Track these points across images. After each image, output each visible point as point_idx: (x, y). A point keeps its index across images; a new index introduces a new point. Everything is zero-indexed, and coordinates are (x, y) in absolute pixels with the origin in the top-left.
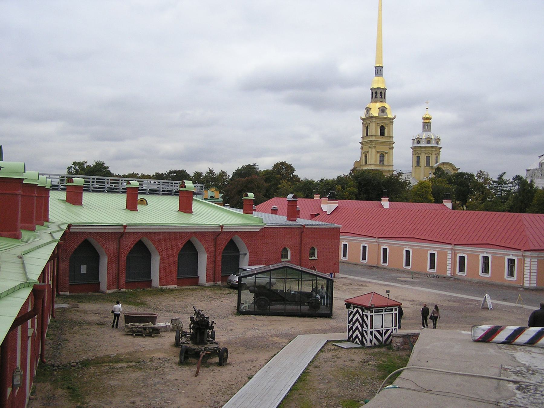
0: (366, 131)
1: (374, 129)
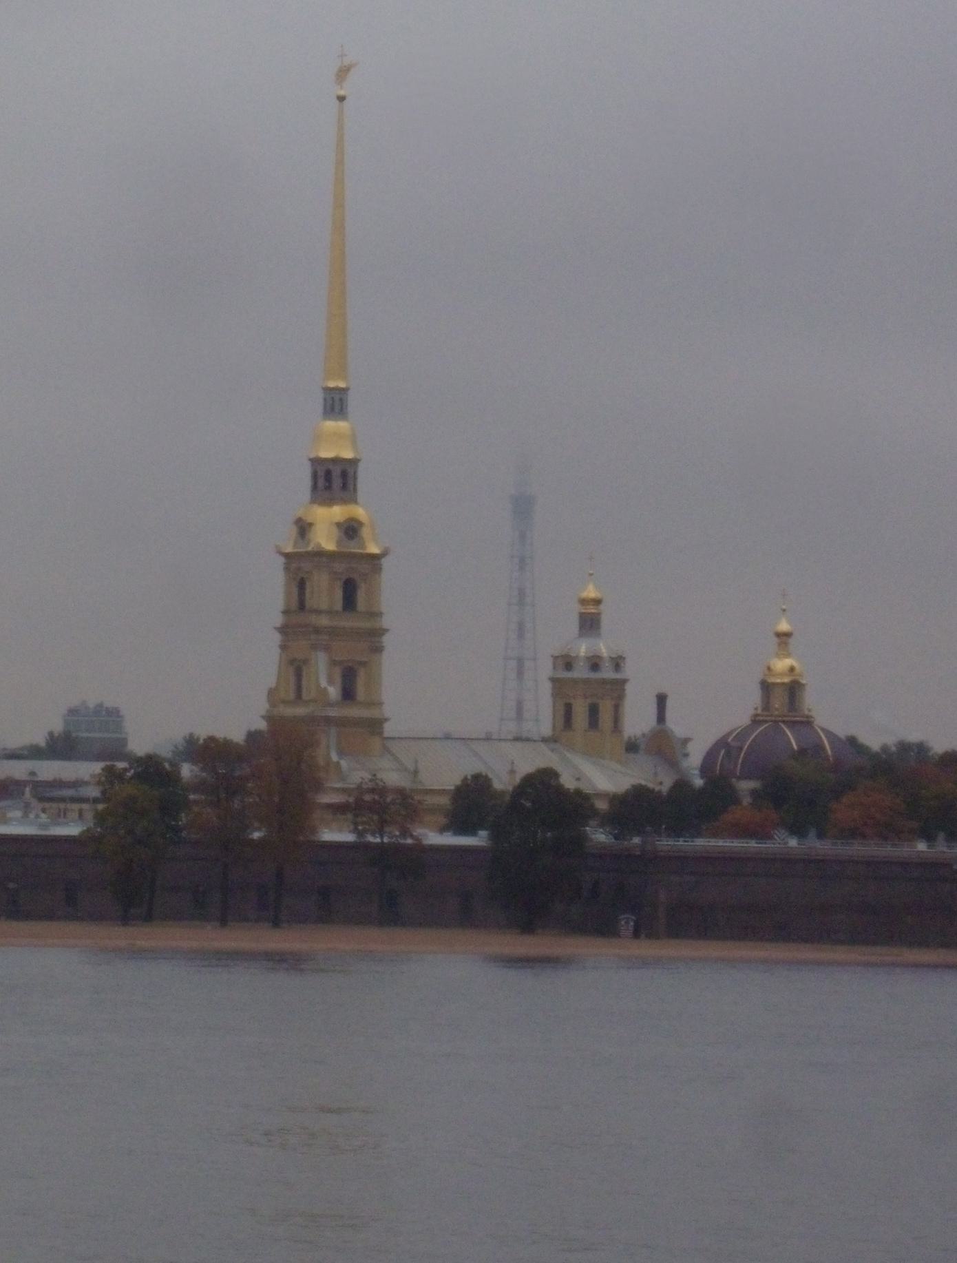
0: (295, 590)
1: (324, 593)
